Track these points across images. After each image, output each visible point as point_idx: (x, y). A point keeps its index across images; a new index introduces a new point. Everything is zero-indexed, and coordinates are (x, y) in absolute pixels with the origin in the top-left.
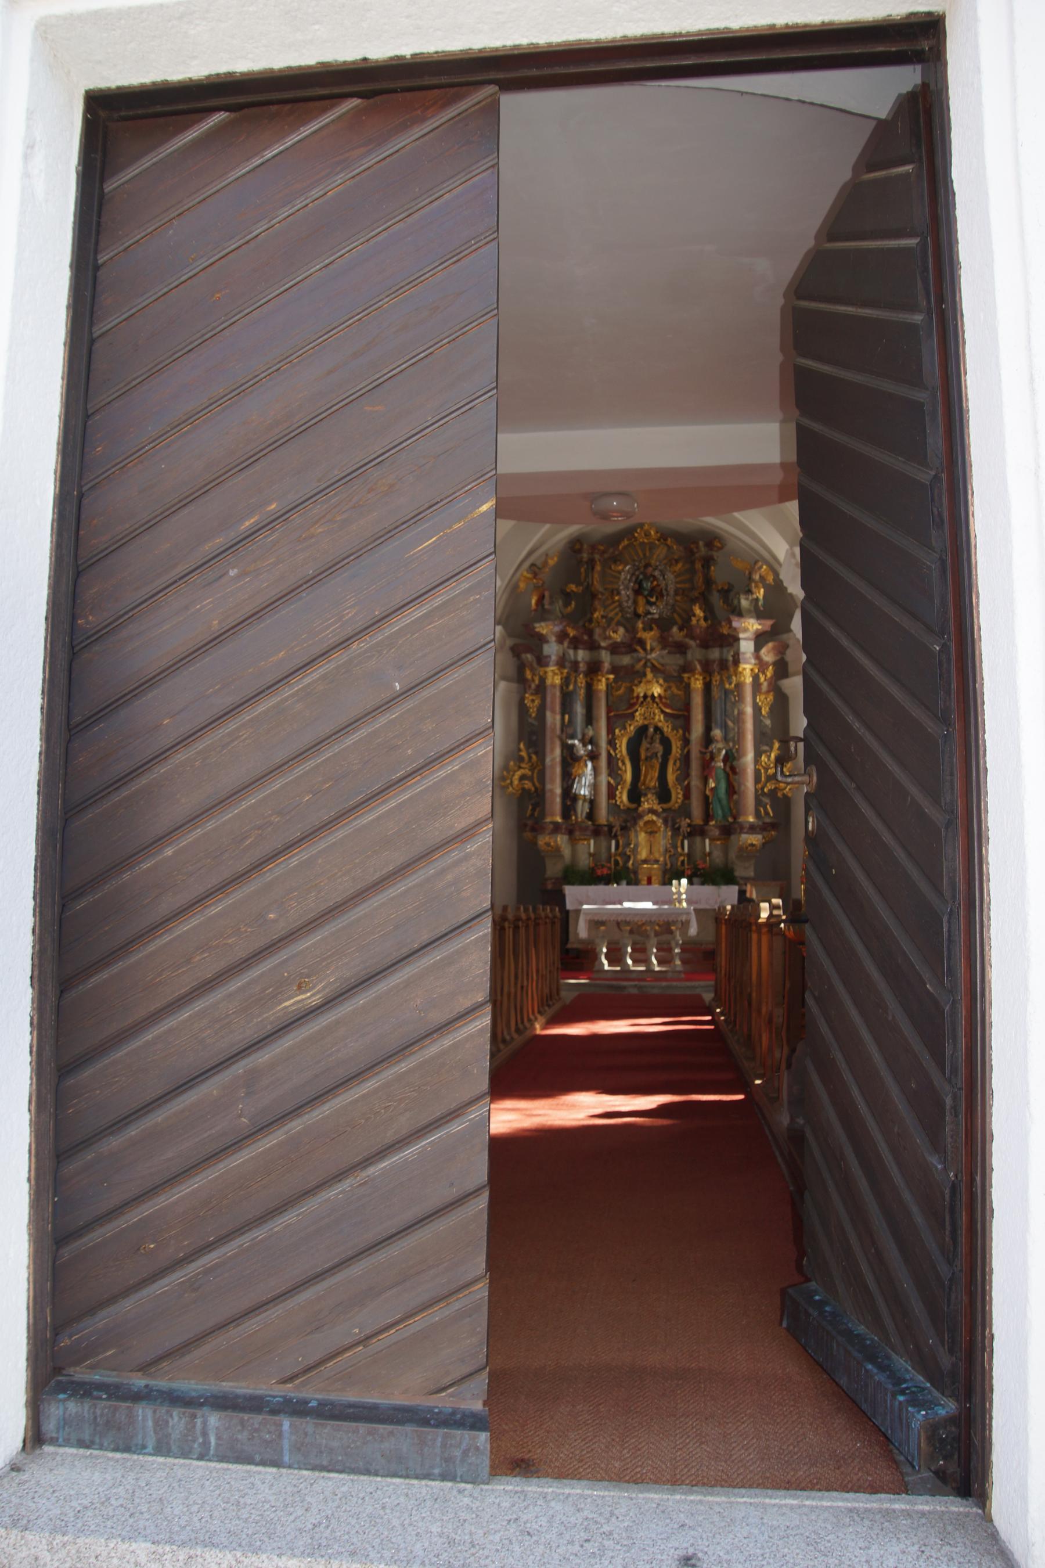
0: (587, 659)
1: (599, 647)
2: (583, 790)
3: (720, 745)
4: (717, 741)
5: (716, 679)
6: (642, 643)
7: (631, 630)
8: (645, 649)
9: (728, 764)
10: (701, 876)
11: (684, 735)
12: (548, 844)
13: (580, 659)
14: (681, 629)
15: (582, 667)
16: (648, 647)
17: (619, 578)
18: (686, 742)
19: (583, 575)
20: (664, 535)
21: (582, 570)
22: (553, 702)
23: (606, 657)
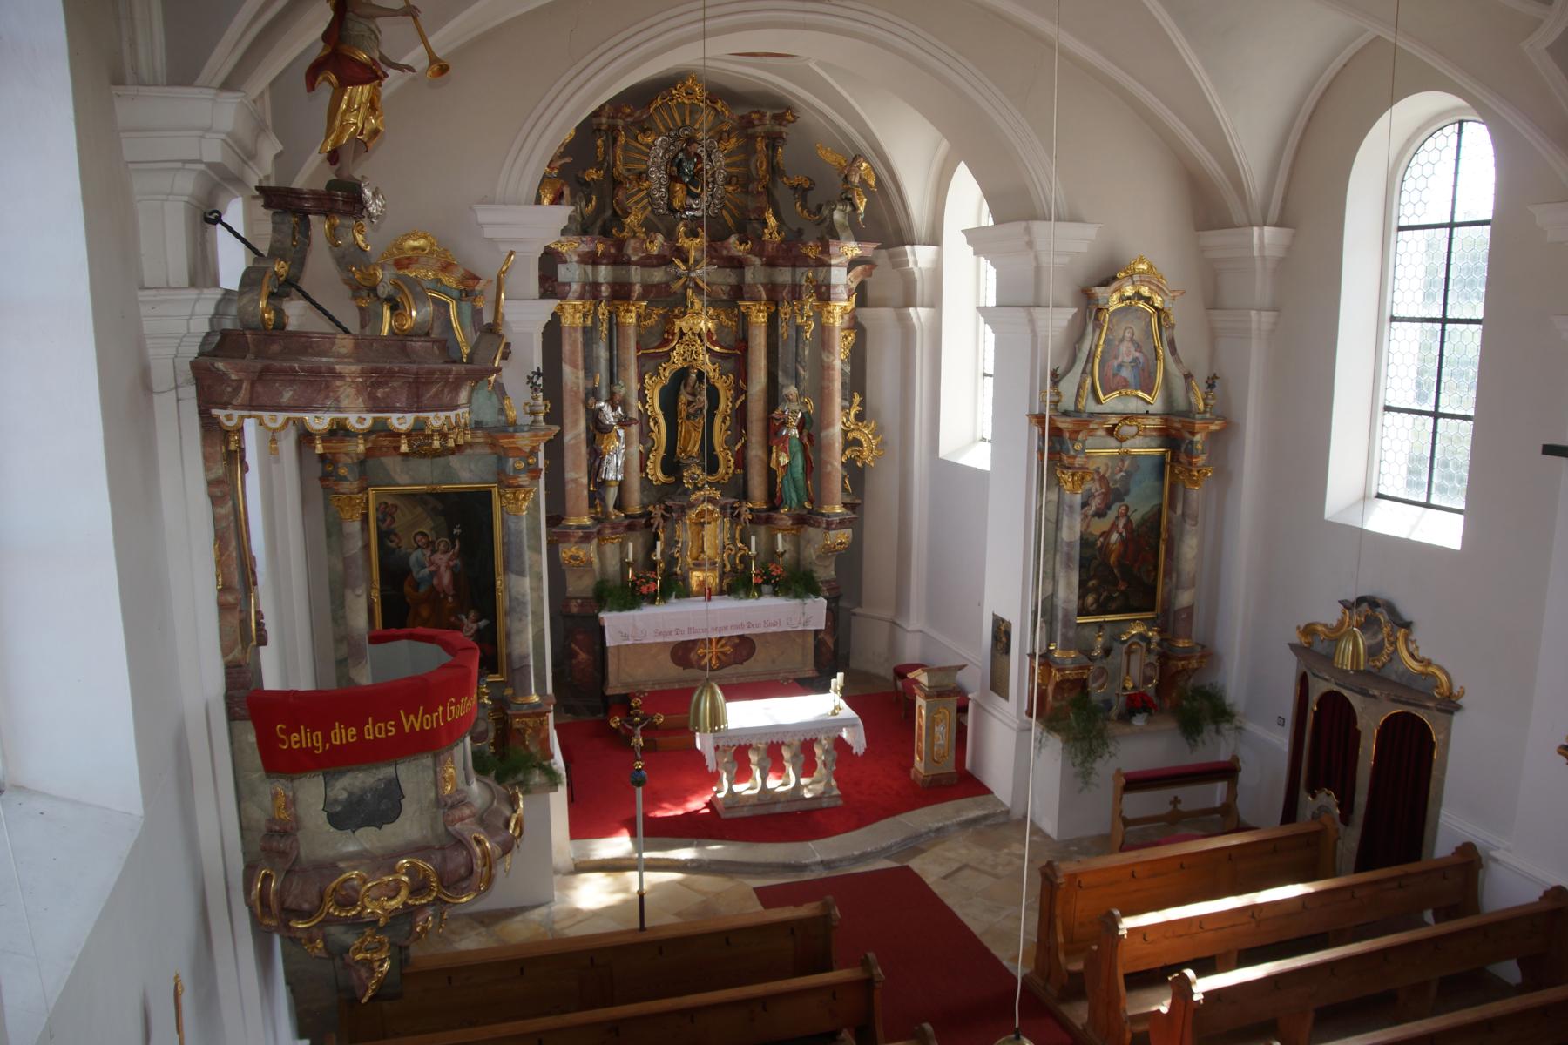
0: (609, 279)
1: (629, 263)
2: (612, 470)
3: (795, 407)
5: (785, 310)
6: (683, 255)
7: (670, 235)
8: (685, 261)
9: (805, 432)
11: (736, 382)
12: (575, 558)
13: (601, 280)
14: (742, 241)
15: (605, 291)
16: (691, 261)
17: (647, 155)
18: (740, 391)
19: (601, 151)
21: (599, 142)
22: (573, 352)
23: (636, 275)
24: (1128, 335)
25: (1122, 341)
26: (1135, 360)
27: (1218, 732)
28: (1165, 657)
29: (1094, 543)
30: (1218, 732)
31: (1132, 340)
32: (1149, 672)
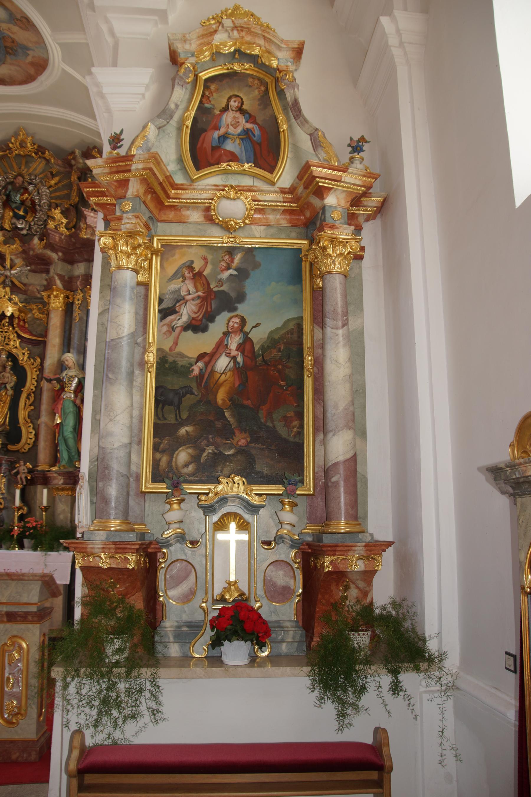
4: (70, 368)
10: (31, 537)
20: (40, 150)
24: (234, 104)
25: (226, 109)
26: (247, 132)
27: (396, 688)
28: (309, 554)
29: (187, 370)
30: (396, 688)
31: (241, 110)
32: (281, 578)
